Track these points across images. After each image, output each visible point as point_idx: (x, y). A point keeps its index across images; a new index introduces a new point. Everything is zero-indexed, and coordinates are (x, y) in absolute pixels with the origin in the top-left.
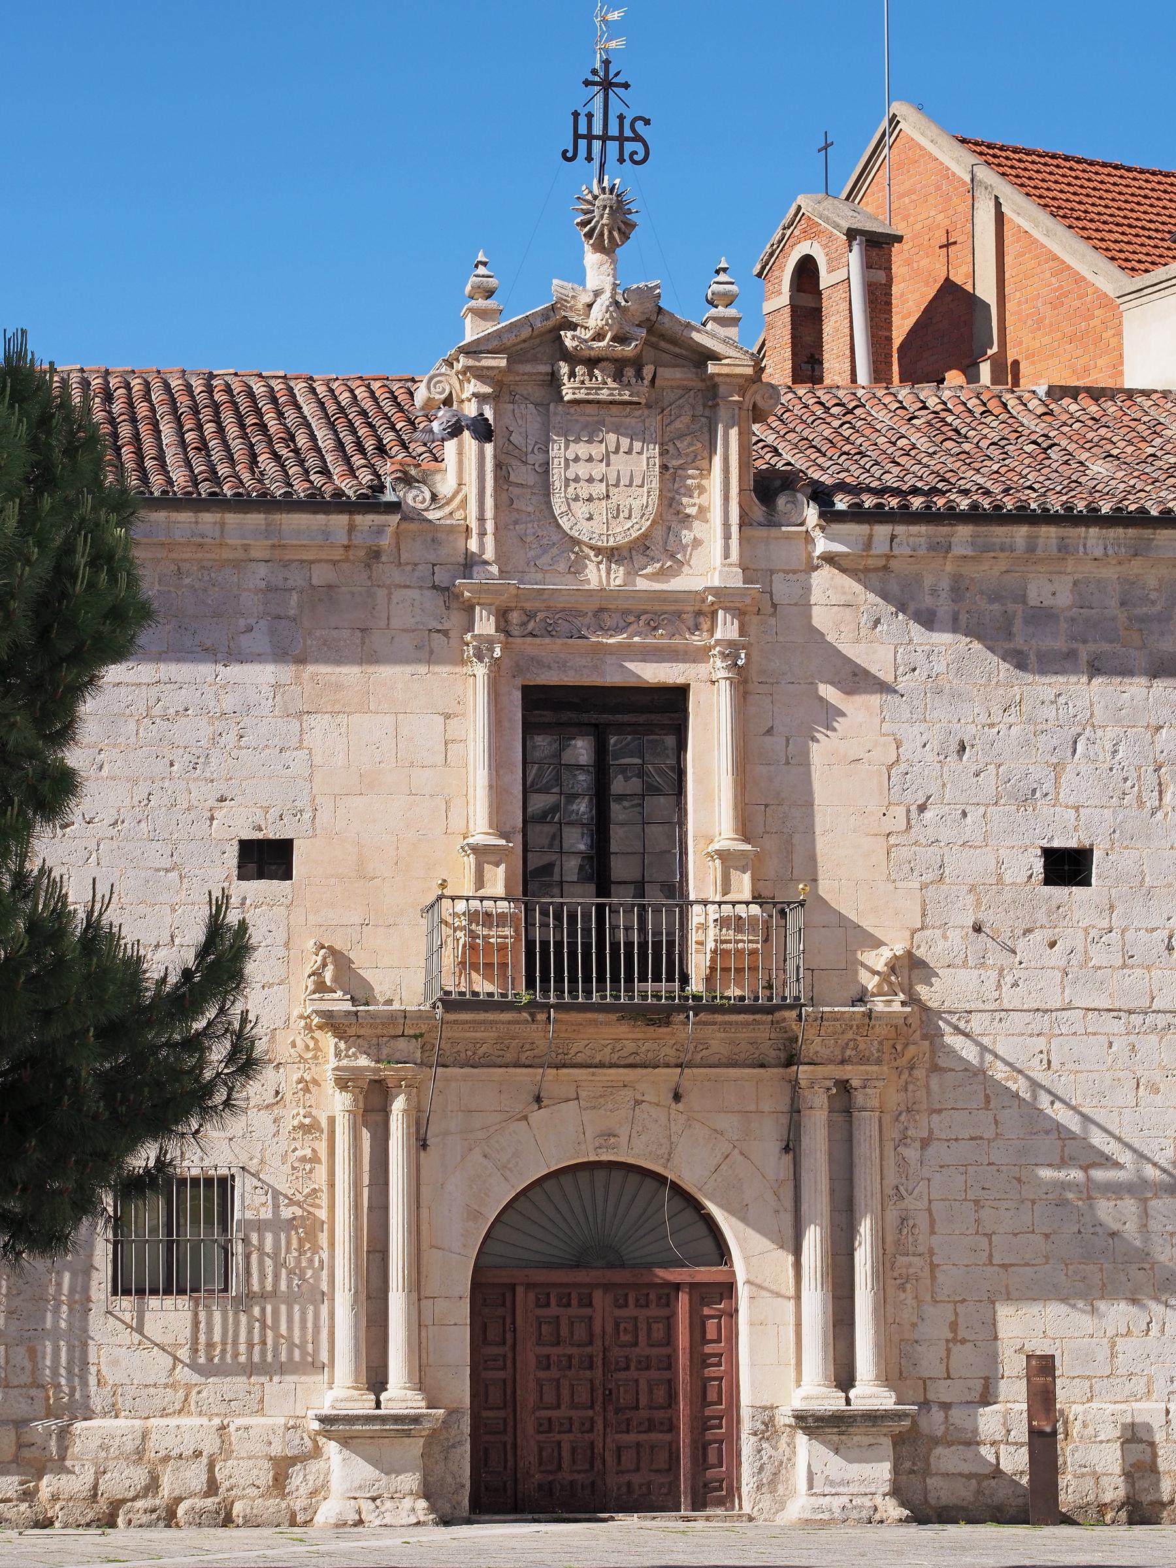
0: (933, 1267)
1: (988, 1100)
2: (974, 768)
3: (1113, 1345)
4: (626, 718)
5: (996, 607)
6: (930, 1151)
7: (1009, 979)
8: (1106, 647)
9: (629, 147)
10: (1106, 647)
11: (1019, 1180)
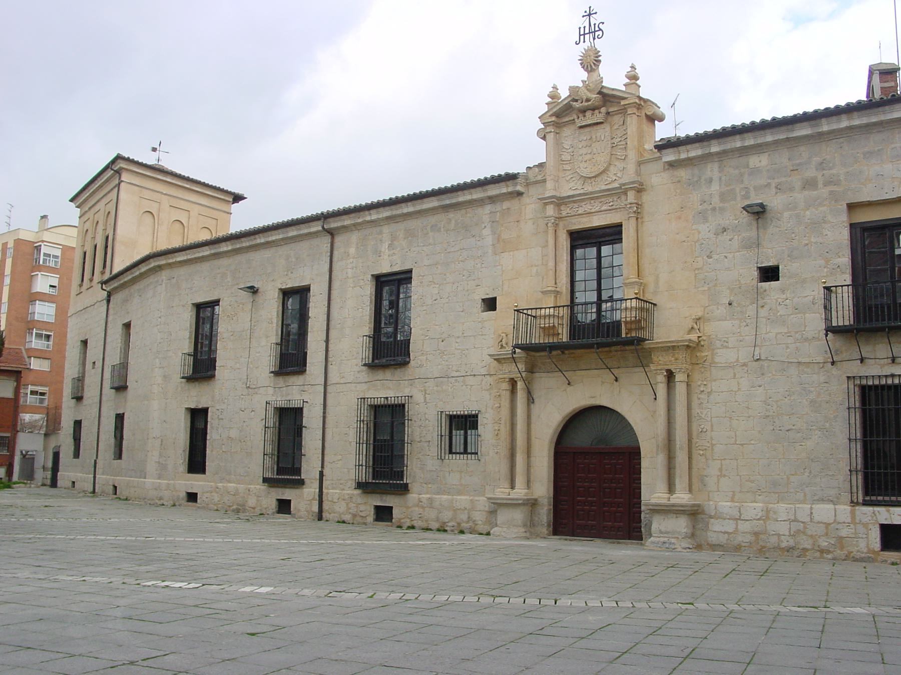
0: (713, 445)
1: (735, 376)
2: (729, 237)
3: (788, 478)
4: (607, 239)
5: (737, 172)
6: (712, 397)
7: (745, 324)
8: (784, 179)
9: (597, 33)
10: (784, 179)
11: (748, 408)
